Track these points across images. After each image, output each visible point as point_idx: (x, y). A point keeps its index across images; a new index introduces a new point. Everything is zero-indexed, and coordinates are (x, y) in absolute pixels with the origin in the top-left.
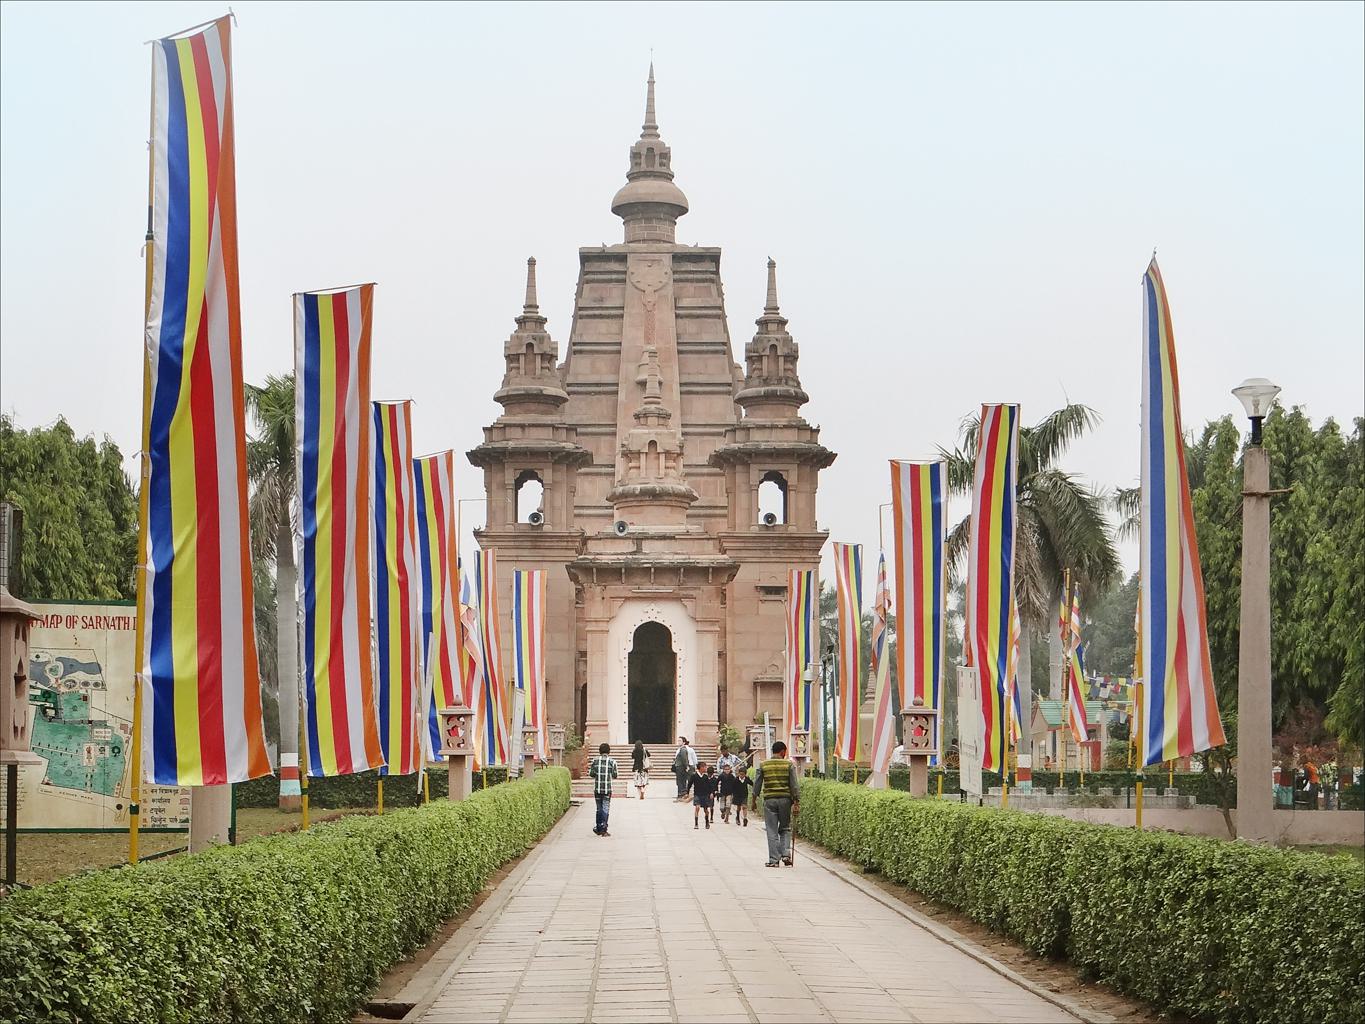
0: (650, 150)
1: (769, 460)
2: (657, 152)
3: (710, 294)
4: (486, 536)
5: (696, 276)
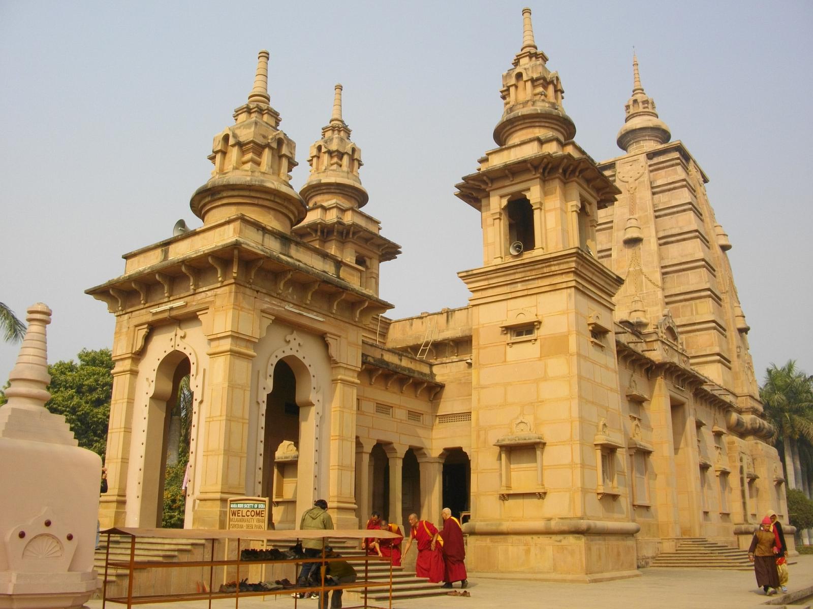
1: (507, 183)
3: (676, 173)
5: (665, 165)
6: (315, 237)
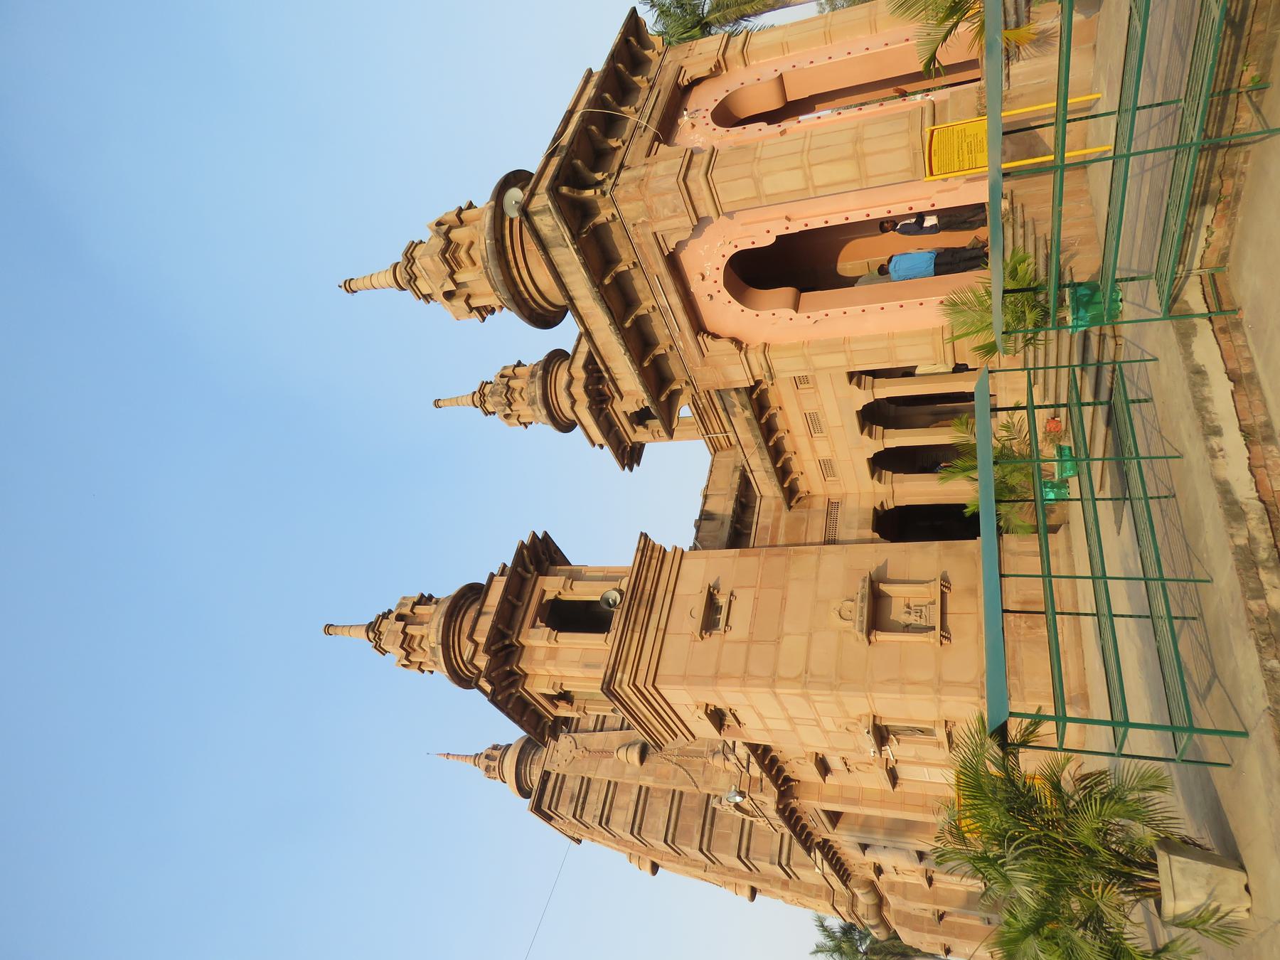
0: (487, 757)
2: (489, 752)
4: (614, 672)
6: (533, 575)
